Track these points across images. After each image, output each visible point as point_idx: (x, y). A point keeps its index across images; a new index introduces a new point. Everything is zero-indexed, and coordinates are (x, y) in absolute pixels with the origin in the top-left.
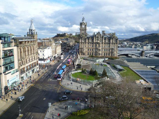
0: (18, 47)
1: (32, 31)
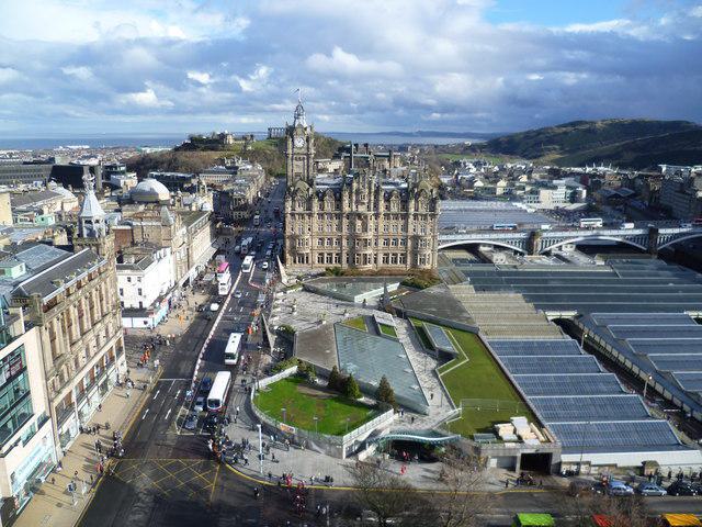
0: (40, 326)
1: (90, 222)
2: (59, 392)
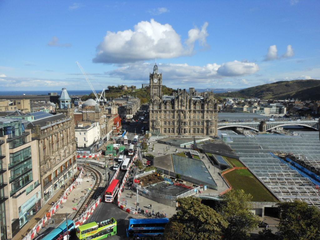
0: (39, 140)
1: (64, 102)
2: (46, 173)
